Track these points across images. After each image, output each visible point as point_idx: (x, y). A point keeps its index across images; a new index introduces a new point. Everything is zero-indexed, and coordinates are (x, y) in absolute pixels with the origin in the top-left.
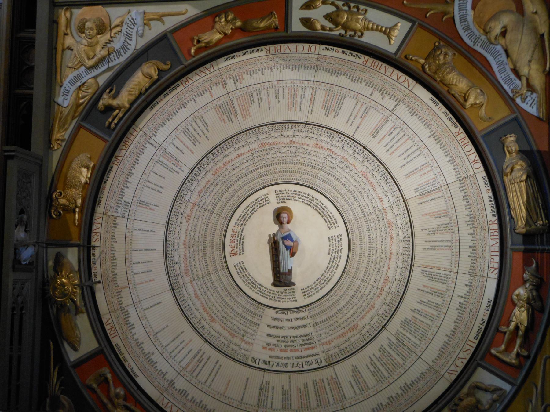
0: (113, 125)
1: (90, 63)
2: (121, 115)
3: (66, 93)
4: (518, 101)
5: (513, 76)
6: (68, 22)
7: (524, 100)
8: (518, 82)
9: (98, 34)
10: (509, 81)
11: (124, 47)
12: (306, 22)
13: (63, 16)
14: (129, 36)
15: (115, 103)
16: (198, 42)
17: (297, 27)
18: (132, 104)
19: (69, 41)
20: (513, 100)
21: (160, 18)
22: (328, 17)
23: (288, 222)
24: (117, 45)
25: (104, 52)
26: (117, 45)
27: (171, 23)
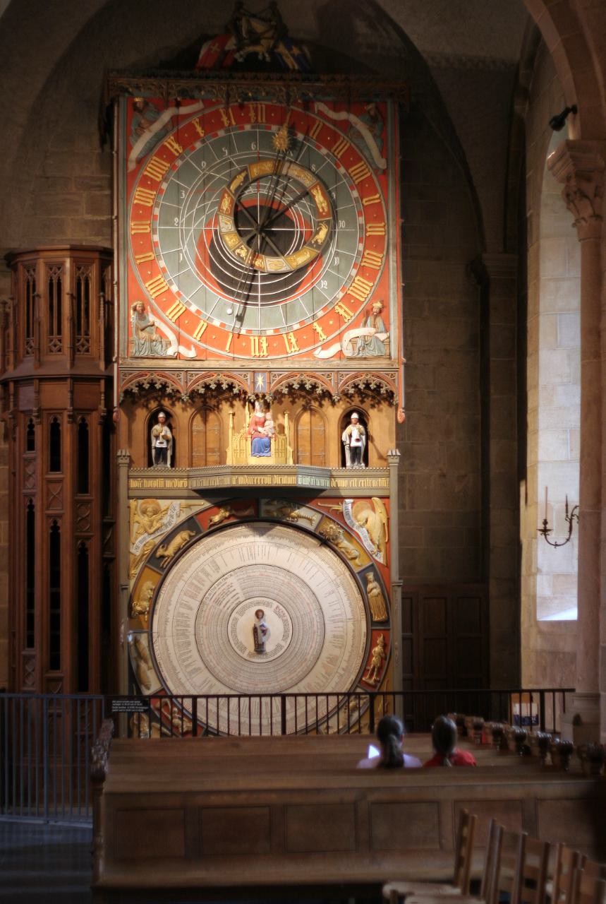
0: (165, 566)
1: (152, 531)
2: (169, 560)
3: (137, 548)
4: (374, 556)
5: (371, 544)
6: (136, 507)
7: (376, 556)
8: (373, 546)
9: (154, 514)
10: (370, 546)
11: (169, 523)
12: (268, 512)
13: (133, 503)
14: (172, 516)
15: (166, 553)
16: (211, 521)
17: (263, 515)
18: (175, 553)
19: (137, 518)
20: (371, 556)
21: (189, 507)
22: (280, 510)
23: (262, 617)
24: (165, 521)
25: (158, 525)
26: (165, 521)
27: (195, 510)
